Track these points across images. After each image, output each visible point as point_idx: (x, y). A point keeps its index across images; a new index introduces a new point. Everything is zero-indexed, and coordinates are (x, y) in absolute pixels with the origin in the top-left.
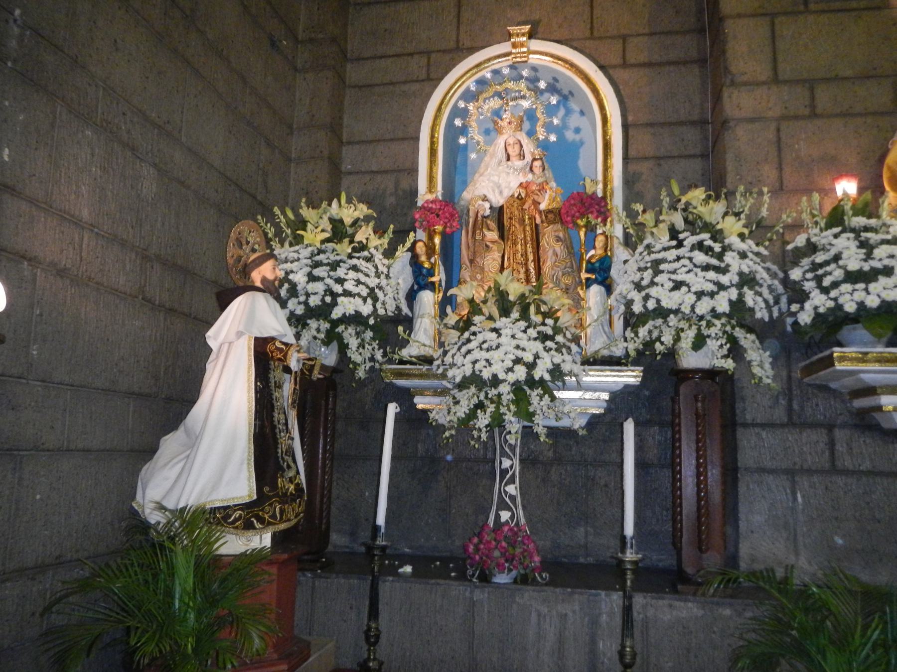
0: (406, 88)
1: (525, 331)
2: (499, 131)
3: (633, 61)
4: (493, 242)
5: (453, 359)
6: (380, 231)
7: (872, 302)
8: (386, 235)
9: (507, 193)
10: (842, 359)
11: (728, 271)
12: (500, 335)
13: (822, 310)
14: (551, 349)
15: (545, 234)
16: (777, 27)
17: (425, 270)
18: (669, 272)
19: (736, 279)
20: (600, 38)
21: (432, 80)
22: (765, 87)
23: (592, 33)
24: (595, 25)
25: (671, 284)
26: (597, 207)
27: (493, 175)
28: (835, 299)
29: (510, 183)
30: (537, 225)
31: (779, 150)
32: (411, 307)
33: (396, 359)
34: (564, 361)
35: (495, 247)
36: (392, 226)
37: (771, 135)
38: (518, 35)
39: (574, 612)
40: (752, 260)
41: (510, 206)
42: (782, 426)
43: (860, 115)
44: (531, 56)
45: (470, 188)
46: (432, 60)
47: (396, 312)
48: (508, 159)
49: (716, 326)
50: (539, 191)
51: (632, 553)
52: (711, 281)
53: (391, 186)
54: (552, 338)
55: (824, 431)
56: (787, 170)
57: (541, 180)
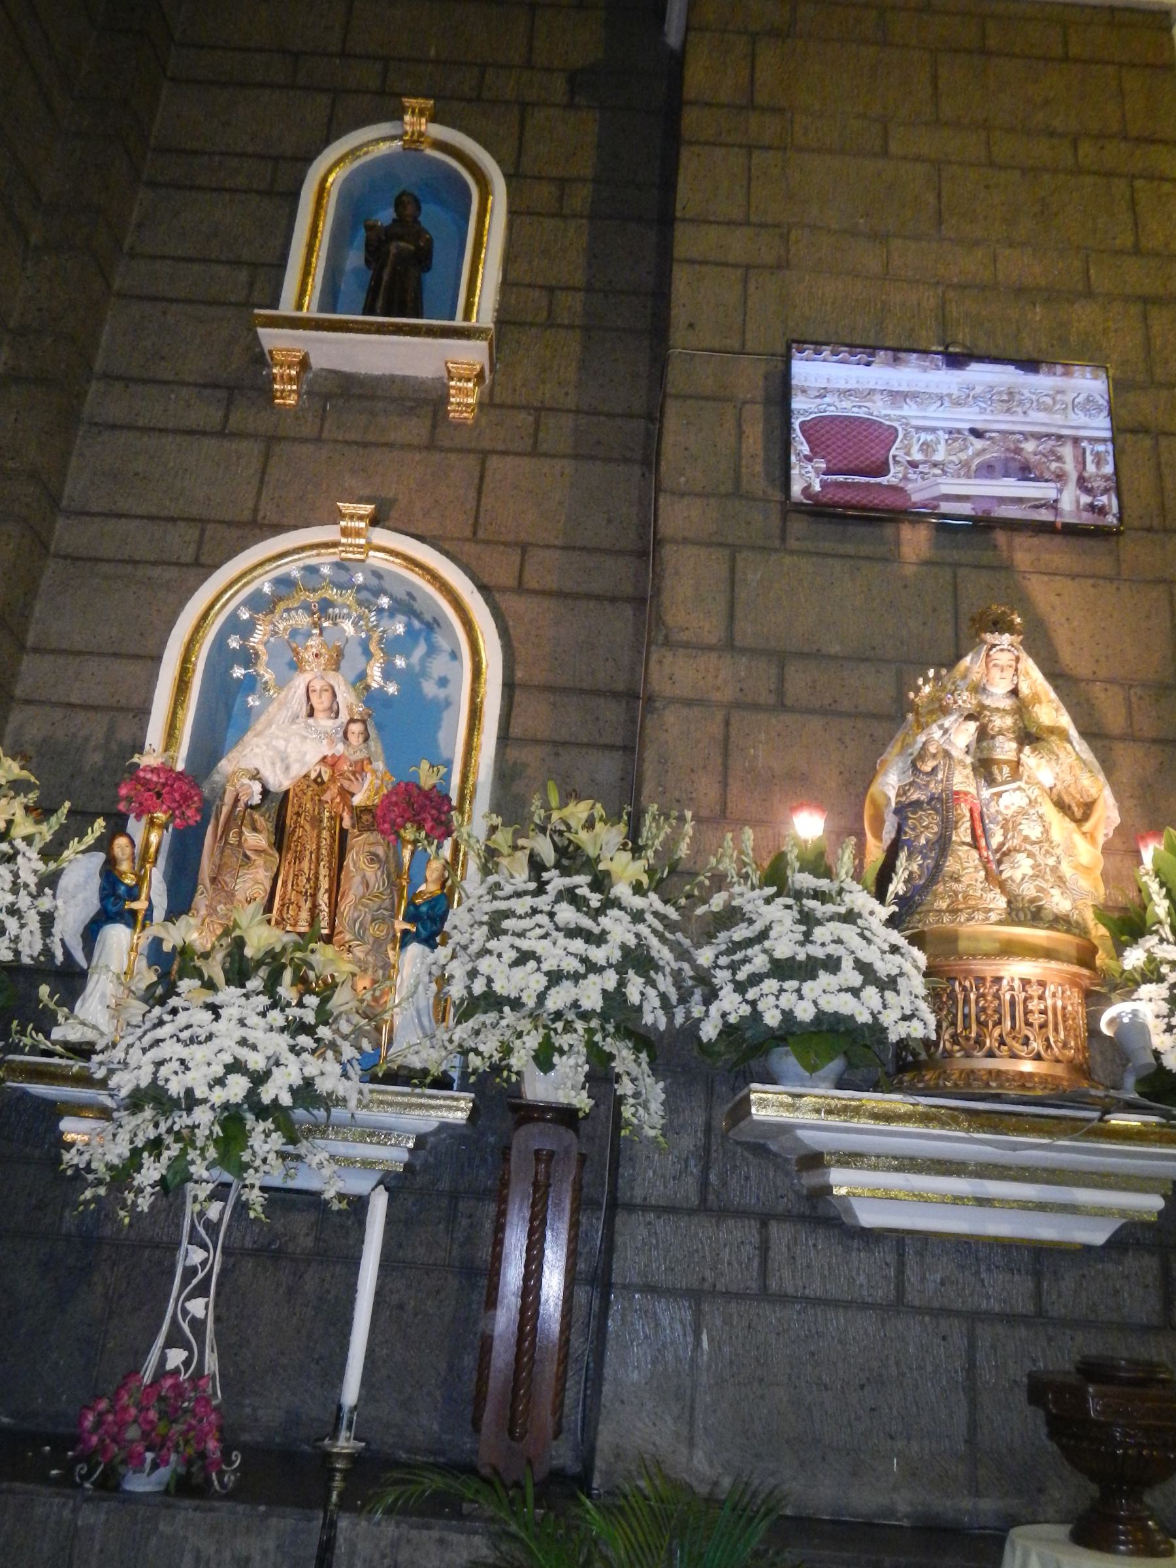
0: (157, 572)
1: (263, 1014)
2: (296, 666)
3: (534, 585)
4: (258, 852)
5: (127, 1054)
6: (41, 812)
7: (805, 1012)
8: (53, 819)
9: (297, 771)
10: (763, 1104)
11: (606, 942)
12: (217, 1017)
13: (732, 1019)
14: (304, 1049)
16: (740, 564)
17: (123, 888)
18: (515, 934)
19: (617, 955)
20: (487, 542)
21: (203, 566)
22: (714, 655)
23: (475, 533)
24: (481, 520)
25: (514, 955)
26: (433, 812)
27: (277, 737)
28: (753, 1004)
29: (305, 754)
30: (341, 828)
31: (726, 754)
32: (89, 953)
33: (25, 1045)
34: (322, 1074)
35: (259, 861)
36: (67, 804)
37: (716, 729)
38: (352, 517)
39: (265, 1553)
40: (650, 926)
41: (300, 794)
42: (691, 1212)
43: (849, 715)
44: (371, 553)
45: (233, 755)
46: (208, 534)
47: (42, 958)
48: (311, 713)
49: (576, 1031)
50: (354, 773)
51: (348, 1440)
52: (576, 956)
53: (99, 735)
54: (308, 1030)
55: (755, 1224)
56: (735, 787)
57: (359, 756)
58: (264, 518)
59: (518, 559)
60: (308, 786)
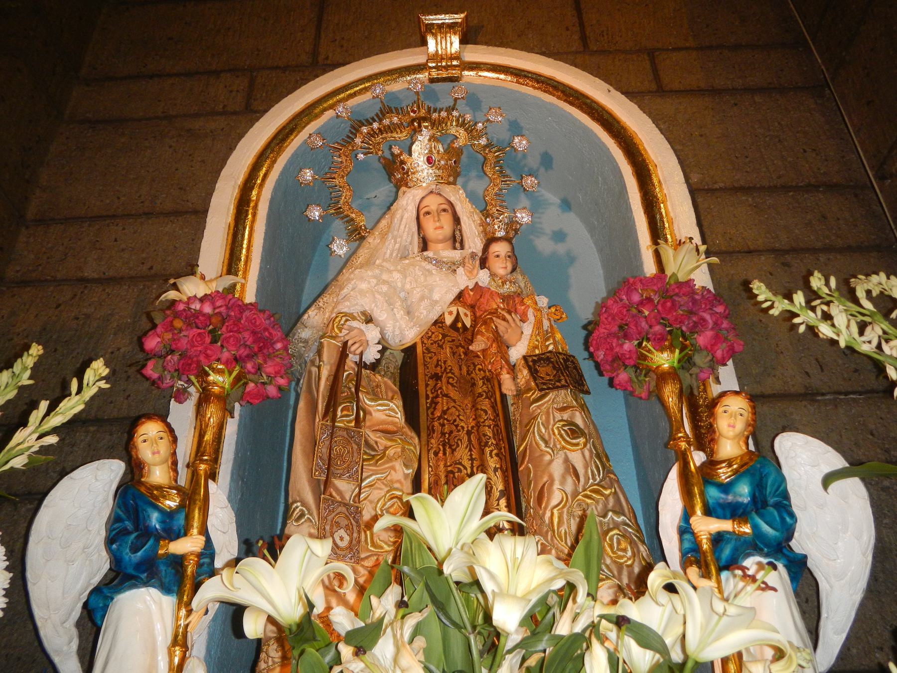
3: (676, 86)
15: (535, 418)
29: (431, 291)
30: (503, 397)
41: (434, 348)
48: (425, 245)
50: (509, 312)
57: (507, 289)
58: (327, 58)
59: (647, 64)
60: (444, 336)
